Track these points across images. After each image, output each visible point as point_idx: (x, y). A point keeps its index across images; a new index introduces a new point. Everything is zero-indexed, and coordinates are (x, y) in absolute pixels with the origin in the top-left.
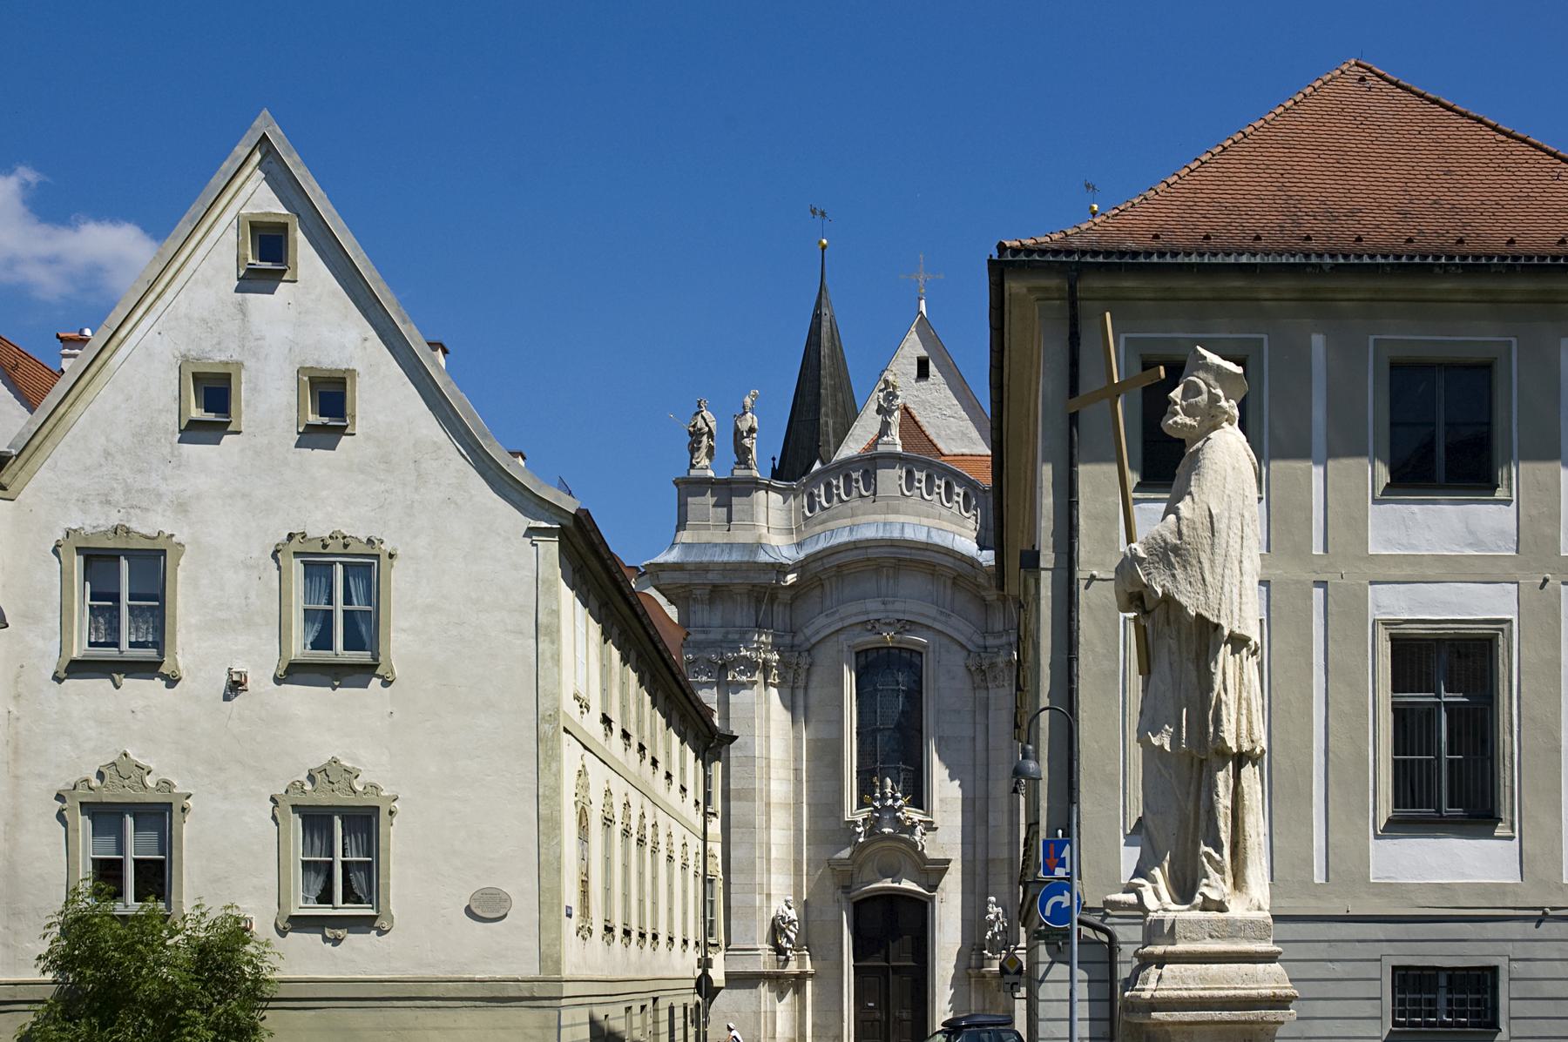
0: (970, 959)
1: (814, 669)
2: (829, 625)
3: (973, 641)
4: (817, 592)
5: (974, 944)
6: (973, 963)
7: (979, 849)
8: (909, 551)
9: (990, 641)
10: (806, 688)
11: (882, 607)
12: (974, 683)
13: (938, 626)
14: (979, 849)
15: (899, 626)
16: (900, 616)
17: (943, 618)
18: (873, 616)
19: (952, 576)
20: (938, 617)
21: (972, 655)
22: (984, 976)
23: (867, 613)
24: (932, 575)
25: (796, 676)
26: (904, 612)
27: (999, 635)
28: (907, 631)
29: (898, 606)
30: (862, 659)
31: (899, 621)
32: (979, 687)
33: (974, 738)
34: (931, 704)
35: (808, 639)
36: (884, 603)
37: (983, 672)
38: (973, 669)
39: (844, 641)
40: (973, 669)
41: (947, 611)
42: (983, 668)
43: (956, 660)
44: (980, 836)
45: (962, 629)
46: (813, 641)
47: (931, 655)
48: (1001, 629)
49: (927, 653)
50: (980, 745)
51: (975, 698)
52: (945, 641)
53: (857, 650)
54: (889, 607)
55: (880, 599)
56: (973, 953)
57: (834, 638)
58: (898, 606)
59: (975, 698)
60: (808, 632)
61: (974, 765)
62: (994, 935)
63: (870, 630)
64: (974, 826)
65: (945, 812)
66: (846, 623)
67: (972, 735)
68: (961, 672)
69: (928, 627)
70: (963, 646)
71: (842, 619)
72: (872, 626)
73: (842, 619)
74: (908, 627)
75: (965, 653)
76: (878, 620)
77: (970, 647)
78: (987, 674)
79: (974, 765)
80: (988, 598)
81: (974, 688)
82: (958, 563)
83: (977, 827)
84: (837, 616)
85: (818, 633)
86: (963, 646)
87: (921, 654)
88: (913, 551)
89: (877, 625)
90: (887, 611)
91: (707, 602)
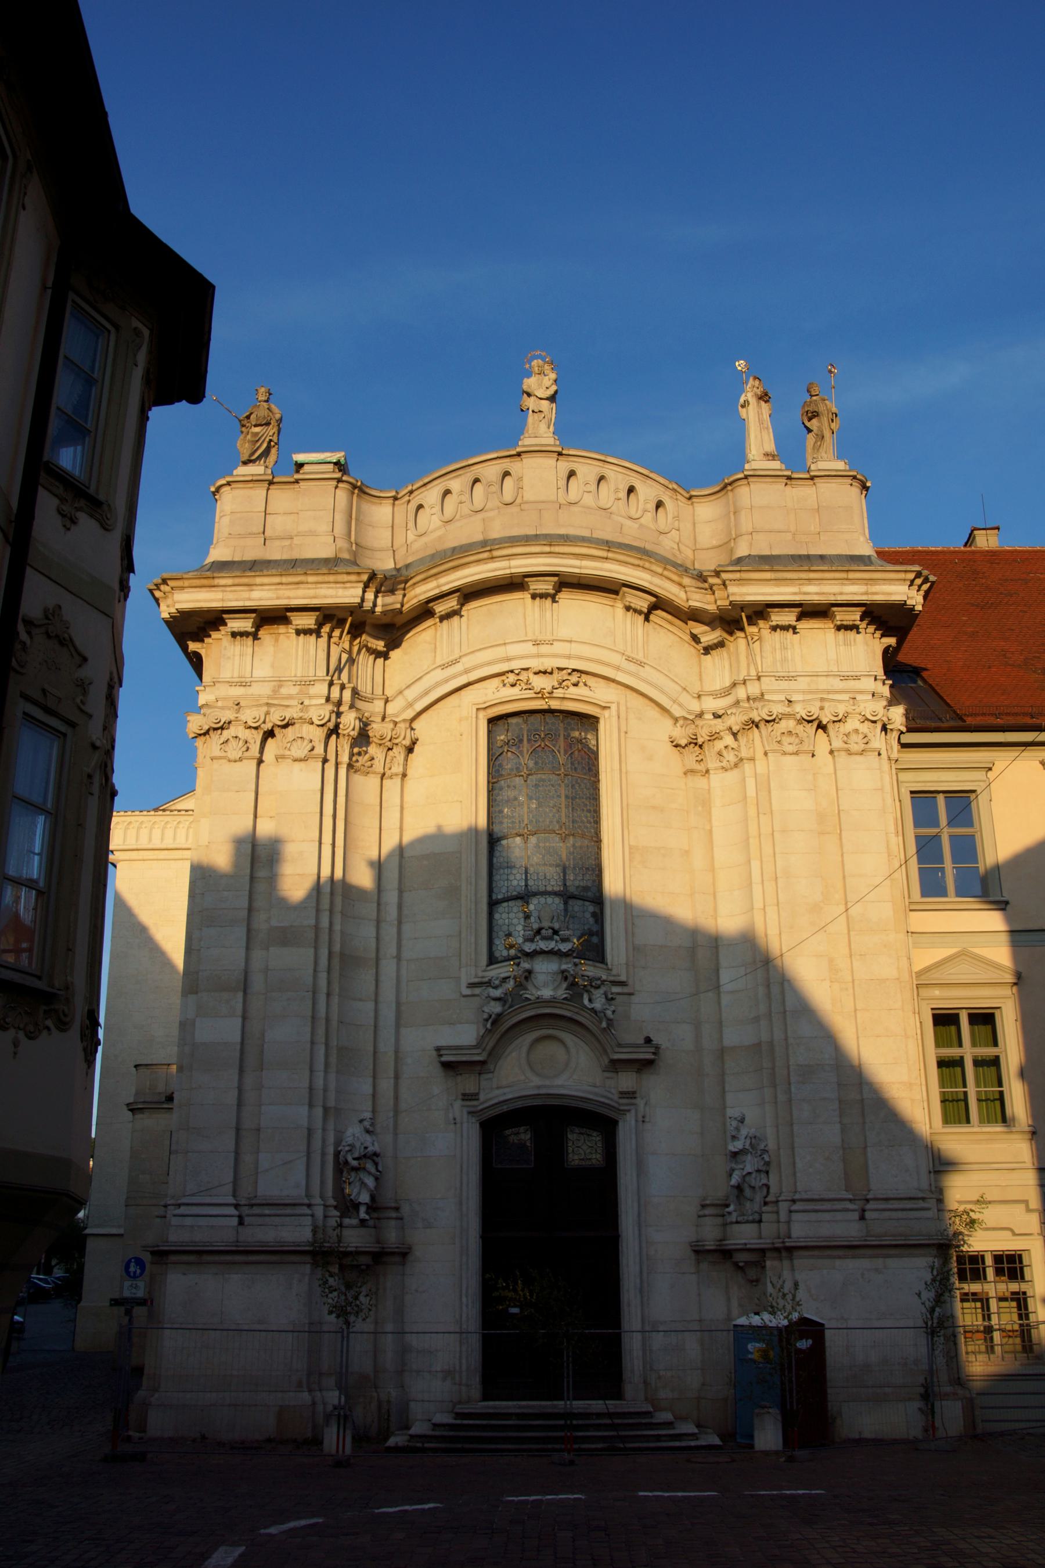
2: (446, 681)
8: (576, 562)
11: (534, 650)
13: (621, 677)
17: (632, 667)
18: (516, 665)
20: (625, 665)
23: (508, 659)
29: (559, 648)
31: (560, 669)
36: (536, 643)
54: (544, 649)
58: (559, 648)
71: (467, 671)
73: (467, 671)
77: (677, 712)
84: (458, 668)
90: (539, 656)
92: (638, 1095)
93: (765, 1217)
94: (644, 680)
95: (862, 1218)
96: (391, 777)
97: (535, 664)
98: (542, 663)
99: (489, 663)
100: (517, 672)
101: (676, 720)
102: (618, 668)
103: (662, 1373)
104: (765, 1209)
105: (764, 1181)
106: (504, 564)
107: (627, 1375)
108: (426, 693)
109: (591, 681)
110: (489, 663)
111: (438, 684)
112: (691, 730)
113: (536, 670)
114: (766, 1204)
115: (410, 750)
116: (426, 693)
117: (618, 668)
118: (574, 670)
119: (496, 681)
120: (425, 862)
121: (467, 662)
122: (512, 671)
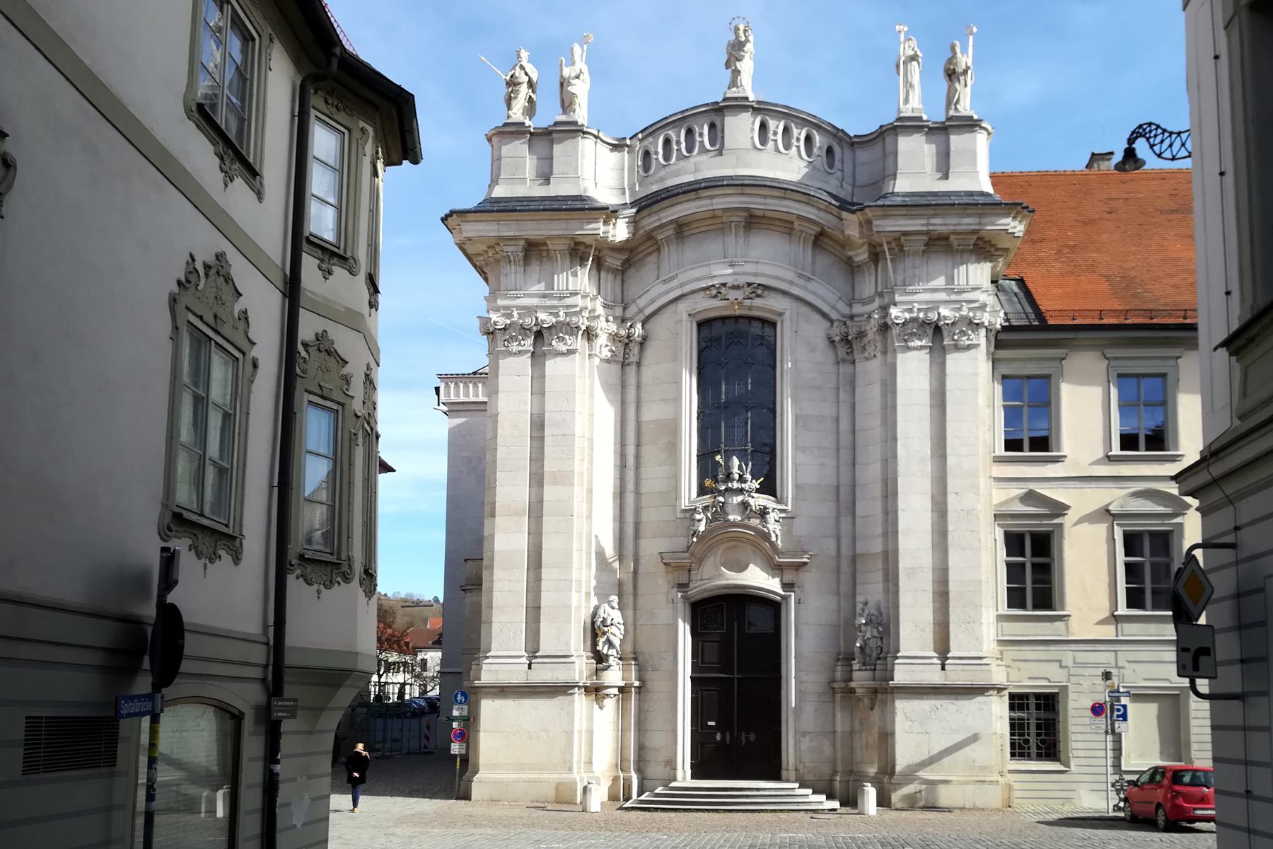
0: (834, 671)
1: (648, 344)
2: (667, 292)
3: (837, 310)
4: (653, 258)
5: (839, 654)
6: (838, 675)
7: (845, 543)
8: (762, 200)
9: (858, 309)
10: (639, 364)
11: (730, 271)
12: (837, 357)
13: (795, 291)
14: (845, 543)
15: (749, 290)
16: (751, 279)
17: (802, 282)
18: (716, 282)
19: (813, 233)
21: (836, 324)
22: (852, 691)
24: (789, 234)
25: (628, 350)
26: (756, 275)
27: (864, 302)
28: (759, 296)
29: (749, 268)
30: (705, 332)
31: (749, 285)
32: (844, 361)
33: (837, 419)
34: (787, 378)
35: (641, 311)
37: (848, 342)
38: (837, 339)
39: (683, 308)
40: (837, 339)
41: (805, 274)
42: (850, 338)
43: (816, 330)
44: (845, 528)
45: (824, 293)
46: (648, 312)
47: (787, 324)
48: (873, 290)
49: (782, 322)
50: (845, 425)
51: (838, 374)
52: (805, 309)
53: (699, 318)
54: (737, 269)
55: (726, 260)
56: (840, 663)
57: (672, 308)
59: (838, 374)
60: (641, 302)
61: (838, 449)
62: (865, 642)
63: (715, 296)
64: (838, 518)
65: (803, 500)
66: (687, 289)
67: (835, 415)
68: (821, 343)
69: (785, 293)
70: (824, 315)
71: (682, 285)
72: (716, 291)
73: (682, 285)
74: (759, 292)
75: (827, 324)
76: (724, 285)
77: (834, 315)
78: (854, 347)
79: (838, 449)
80: (857, 259)
81: (838, 363)
82: (822, 214)
83: (842, 519)
84: (675, 283)
85: (653, 302)
86: (824, 315)
87: (774, 325)
88: (768, 201)
89: (723, 290)
91: (522, 263)
92: (796, 585)
93: (878, 667)
94: (813, 293)
95: (943, 669)
96: (628, 365)
97: (730, 281)
98: (736, 280)
99: (698, 279)
100: (717, 286)
101: (832, 321)
102: (792, 283)
103: (807, 764)
104: (878, 662)
105: (879, 644)
106: (708, 201)
107: (784, 764)
108: (653, 301)
109: (773, 294)
110: (698, 279)
111: (661, 295)
112: (843, 329)
113: (729, 285)
114: (879, 659)
115: (641, 344)
116: (653, 301)
117: (792, 283)
118: (759, 285)
119: (702, 294)
120: (653, 426)
121: (683, 278)
122: (714, 286)
